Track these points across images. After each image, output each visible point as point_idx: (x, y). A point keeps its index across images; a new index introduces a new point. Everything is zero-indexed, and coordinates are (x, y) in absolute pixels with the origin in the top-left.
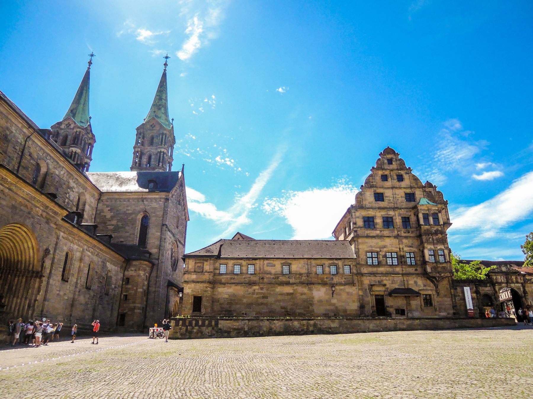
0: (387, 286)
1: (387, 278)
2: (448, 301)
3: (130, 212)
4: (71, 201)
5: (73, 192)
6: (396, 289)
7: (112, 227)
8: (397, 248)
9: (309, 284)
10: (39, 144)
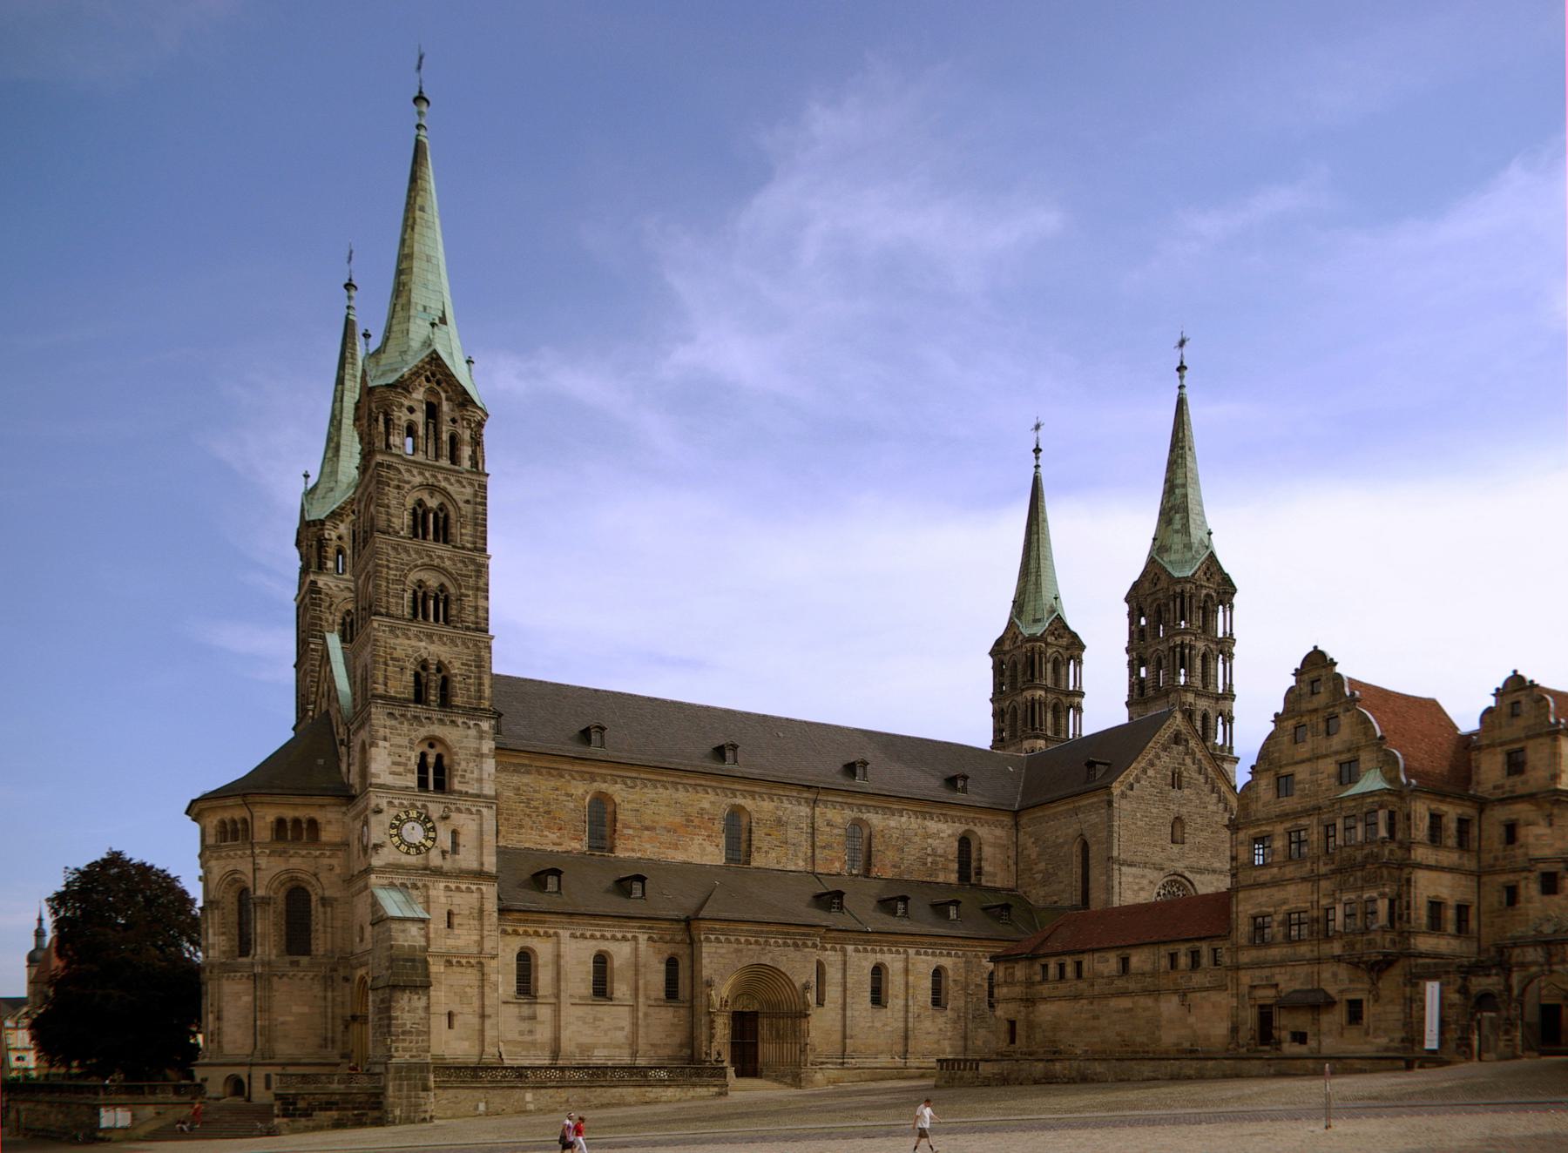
0: (1281, 987)
1: (1283, 970)
2: (1394, 1012)
3: (1061, 840)
4: (940, 856)
5: (943, 838)
6: (1296, 991)
7: (1039, 876)
8: (1306, 902)
9: (1155, 993)
10: (840, 800)
